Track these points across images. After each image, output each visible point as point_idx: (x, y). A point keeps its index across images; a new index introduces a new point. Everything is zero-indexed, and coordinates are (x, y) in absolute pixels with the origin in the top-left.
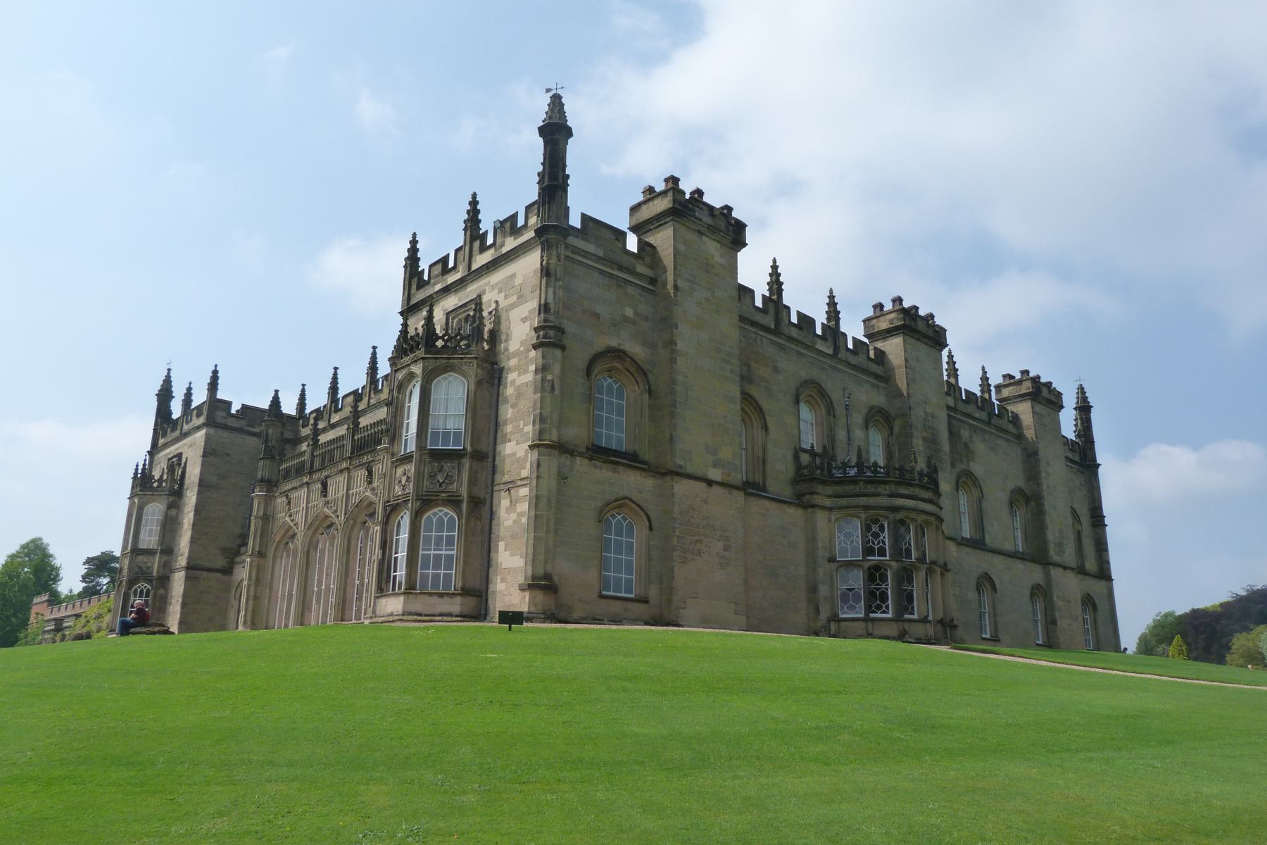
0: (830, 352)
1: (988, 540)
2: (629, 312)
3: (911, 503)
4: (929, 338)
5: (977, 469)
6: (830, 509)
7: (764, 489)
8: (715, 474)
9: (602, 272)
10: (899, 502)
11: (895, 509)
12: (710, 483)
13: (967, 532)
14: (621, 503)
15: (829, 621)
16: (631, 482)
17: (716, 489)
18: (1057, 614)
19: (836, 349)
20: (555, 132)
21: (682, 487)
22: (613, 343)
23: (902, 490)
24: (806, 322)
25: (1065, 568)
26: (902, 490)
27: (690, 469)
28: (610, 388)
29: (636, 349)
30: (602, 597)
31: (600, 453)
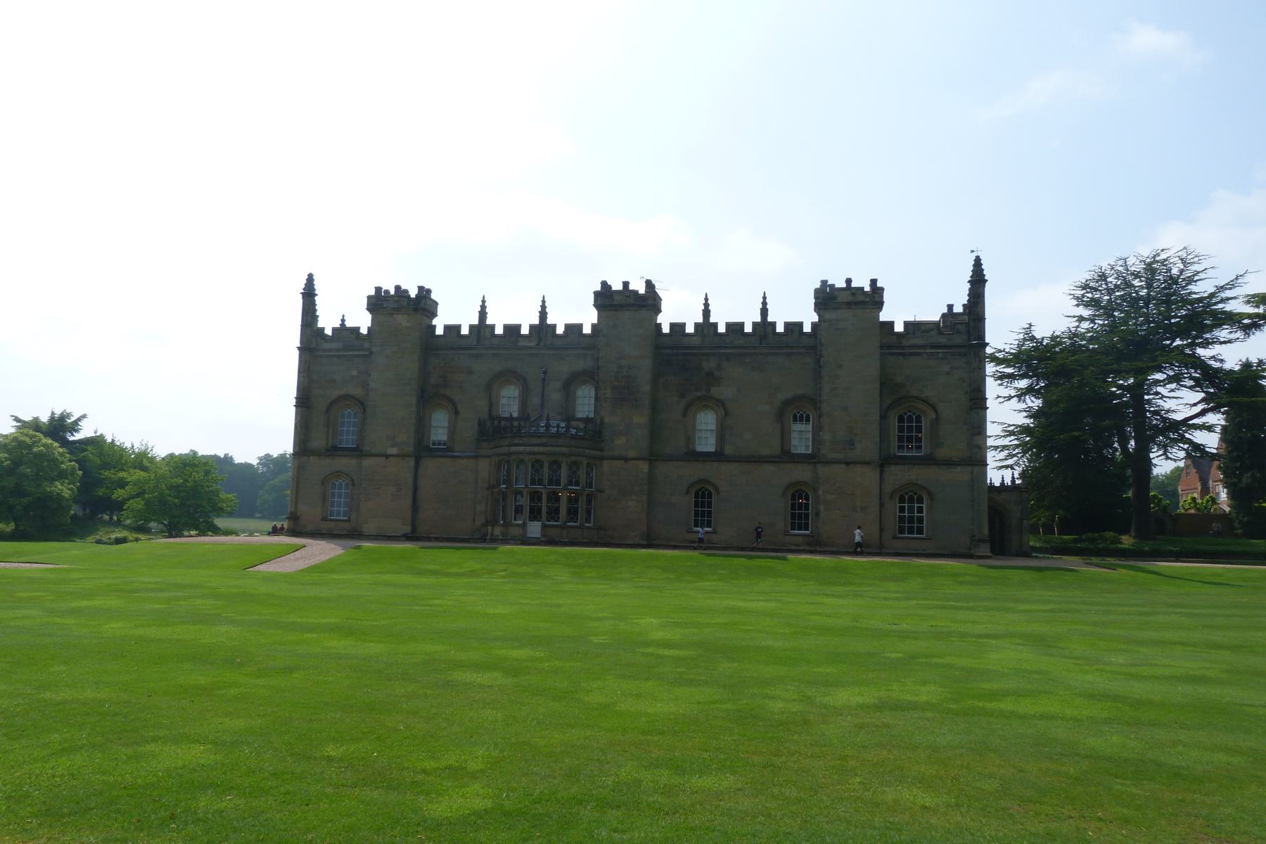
0: (533, 344)
1: (728, 450)
2: (354, 373)
3: (521, 449)
4: (633, 305)
5: (725, 391)
6: (489, 457)
7: (449, 449)
8: (393, 451)
9: (339, 357)
10: (513, 449)
11: (510, 454)
12: (387, 456)
13: (707, 444)
14: (337, 474)
15: (483, 525)
16: (343, 463)
17: (392, 459)
18: (822, 508)
19: (540, 340)
20: (309, 294)
21: (367, 462)
22: (343, 392)
23: (517, 441)
24: (512, 330)
25: (848, 464)
26: (517, 441)
27: (374, 451)
28: (349, 414)
29: (357, 391)
30: (324, 519)
31: (334, 450)
